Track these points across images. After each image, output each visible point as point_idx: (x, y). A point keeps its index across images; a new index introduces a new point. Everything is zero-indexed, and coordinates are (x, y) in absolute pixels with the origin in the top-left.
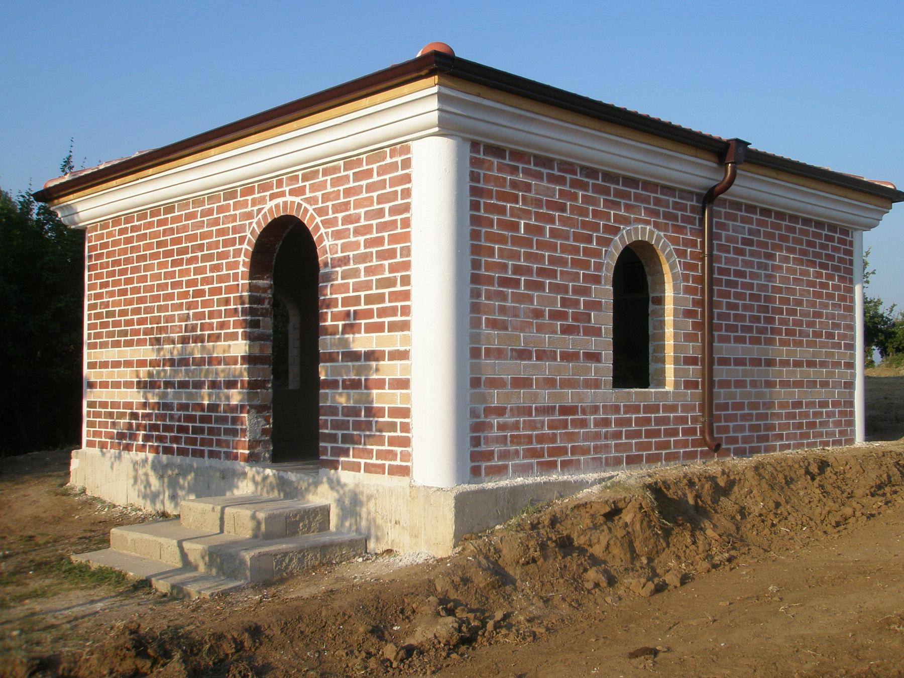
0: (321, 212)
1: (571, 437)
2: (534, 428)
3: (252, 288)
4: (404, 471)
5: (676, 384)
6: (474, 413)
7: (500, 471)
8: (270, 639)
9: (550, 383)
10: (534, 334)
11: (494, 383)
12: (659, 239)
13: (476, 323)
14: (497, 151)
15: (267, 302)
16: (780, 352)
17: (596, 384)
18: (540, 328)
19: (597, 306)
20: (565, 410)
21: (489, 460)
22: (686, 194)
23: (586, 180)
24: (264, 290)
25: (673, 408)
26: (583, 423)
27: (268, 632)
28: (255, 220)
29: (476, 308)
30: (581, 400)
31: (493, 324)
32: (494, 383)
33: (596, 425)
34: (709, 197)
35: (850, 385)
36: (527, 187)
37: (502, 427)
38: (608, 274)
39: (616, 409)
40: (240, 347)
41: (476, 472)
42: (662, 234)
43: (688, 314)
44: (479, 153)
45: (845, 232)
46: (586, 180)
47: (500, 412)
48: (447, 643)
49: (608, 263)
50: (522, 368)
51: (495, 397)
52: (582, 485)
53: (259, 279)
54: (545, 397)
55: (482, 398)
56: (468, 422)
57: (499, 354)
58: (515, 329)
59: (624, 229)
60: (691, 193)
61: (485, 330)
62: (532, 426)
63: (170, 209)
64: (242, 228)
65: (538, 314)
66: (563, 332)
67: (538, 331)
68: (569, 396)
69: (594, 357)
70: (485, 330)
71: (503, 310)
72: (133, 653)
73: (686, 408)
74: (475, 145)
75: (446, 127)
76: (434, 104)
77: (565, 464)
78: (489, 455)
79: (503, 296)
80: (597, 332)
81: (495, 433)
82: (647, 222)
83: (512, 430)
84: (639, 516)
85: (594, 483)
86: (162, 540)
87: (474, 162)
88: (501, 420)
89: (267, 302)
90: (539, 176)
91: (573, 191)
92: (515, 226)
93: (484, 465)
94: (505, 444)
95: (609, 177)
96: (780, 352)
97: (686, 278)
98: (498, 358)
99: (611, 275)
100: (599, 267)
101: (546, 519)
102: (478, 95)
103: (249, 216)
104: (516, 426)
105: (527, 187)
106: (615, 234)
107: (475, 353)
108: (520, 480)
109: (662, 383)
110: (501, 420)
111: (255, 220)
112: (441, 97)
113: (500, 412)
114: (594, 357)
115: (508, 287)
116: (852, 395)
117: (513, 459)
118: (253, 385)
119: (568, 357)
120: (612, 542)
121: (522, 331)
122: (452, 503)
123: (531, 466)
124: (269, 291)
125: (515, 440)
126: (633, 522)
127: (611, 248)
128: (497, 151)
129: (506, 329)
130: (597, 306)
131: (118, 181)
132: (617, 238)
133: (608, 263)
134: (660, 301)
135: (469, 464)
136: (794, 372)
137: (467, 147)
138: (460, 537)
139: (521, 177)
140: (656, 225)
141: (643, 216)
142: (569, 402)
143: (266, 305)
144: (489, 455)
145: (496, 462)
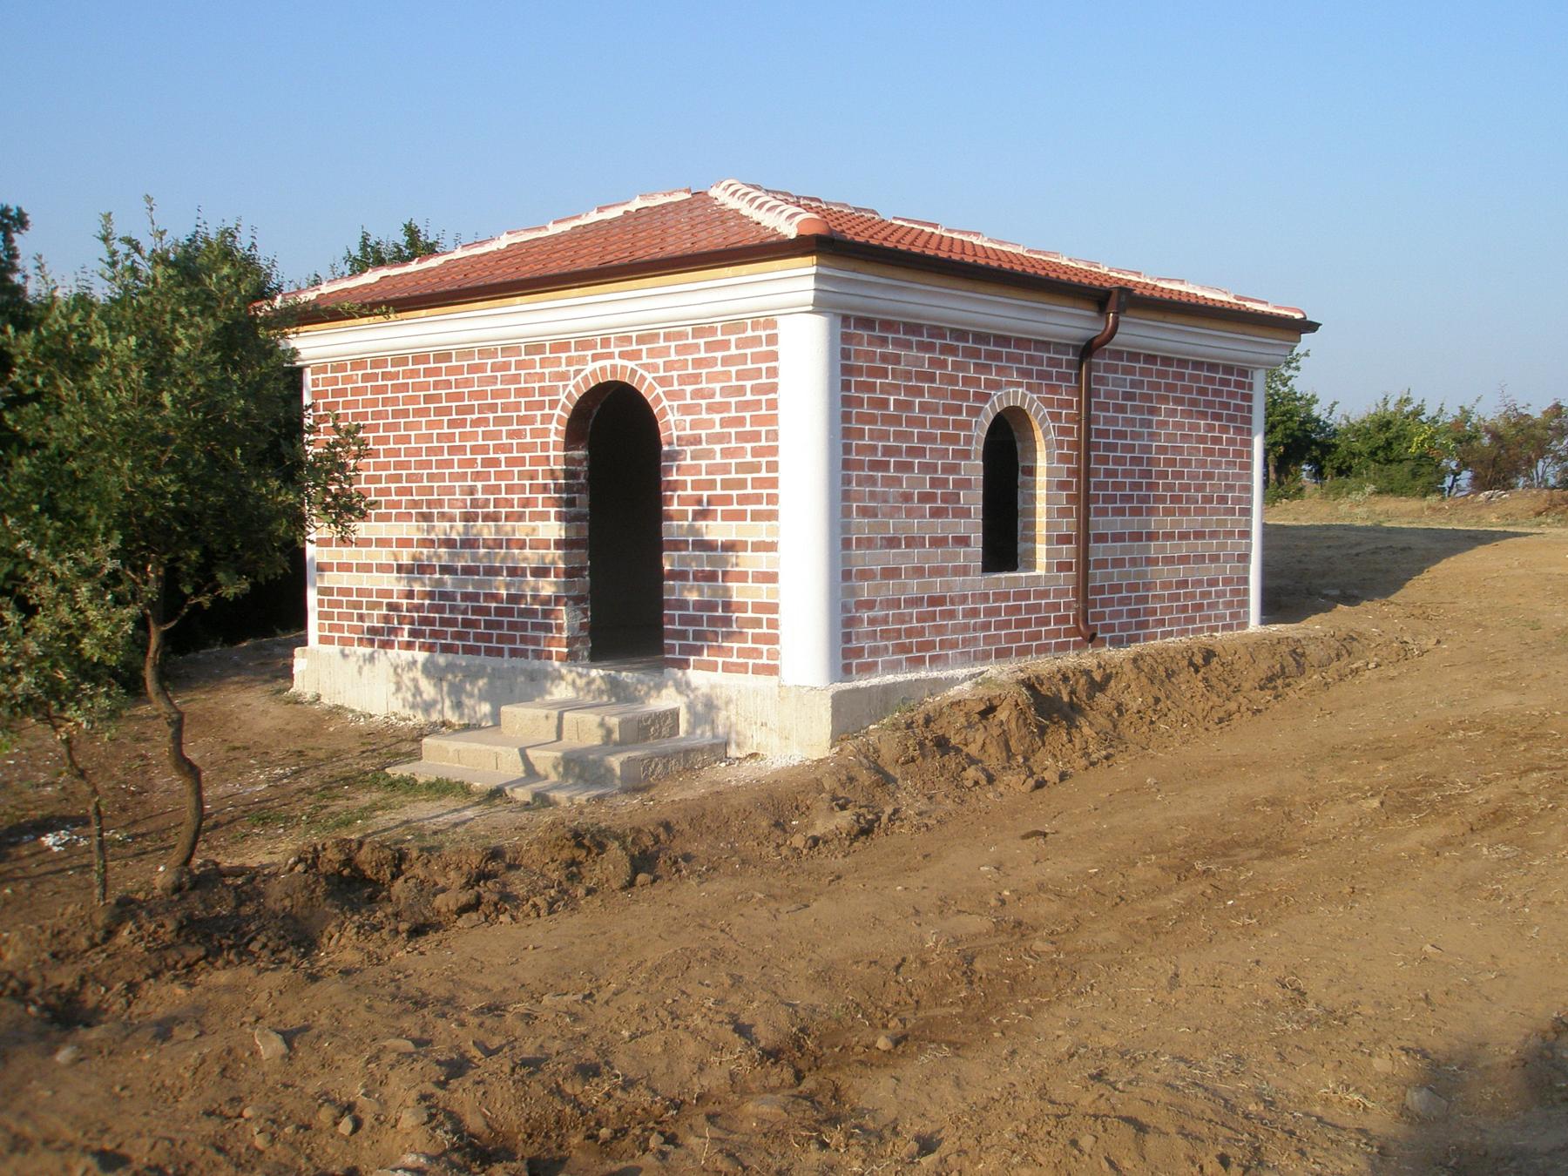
0: (663, 381)
1: (939, 630)
2: (903, 622)
3: (568, 461)
4: (772, 670)
5: (1049, 567)
6: (845, 608)
7: (869, 668)
8: (682, 833)
9: (919, 572)
10: (903, 519)
11: (865, 575)
12: (1032, 401)
13: (847, 512)
14: (866, 323)
15: (582, 475)
17: (965, 571)
18: (909, 513)
20: (934, 601)
21: (860, 657)
22: (1061, 347)
23: (956, 343)
24: (580, 462)
25: (1045, 594)
26: (951, 614)
27: (677, 827)
28: (572, 382)
29: (846, 496)
30: (950, 590)
31: (864, 512)
32: (865, 575)
33: (965, 616)
34: (1087, 350)
35: (1245, 558)
36: (896, 359)
37: (872, 621)
38: (978, 447)
39: (985, 597)
40: (553, 529)
41: (847, 669)
42: (1035, 396)
43: (1063, 485)
44: (849, 327)
46: (956, 343)
47: (870, 605)
48: (848, 834)
50: (891, 557)
51: (865, 590)
52: (952, 682)
53: (574, 449)
54: (914, 587)
55: (851, 592)
56: (840, 617)
57: (868, 543)
58: (884, 516)
59: (995, 395)
60: (1067, 345)
61: (856, 519)
62: (901, 619)
63: (446, 357)
64: (553, 390)
65: (907, 497)
66: (932, 516)
67: (907, 516)
68: (938, 585)
69: (963, 541)
70: (856, 519)
71: (873, 495)
72: (573, 843)
73: (1059, 593)
74: (845, 319)
75: (820, 306)
76: (810, 283)
77: (933, 659)
78: (859, 652)
79: (872, 481)
80: (966, 513)
81: (865, 628)
82: (1019, 385)
83: (881, 625)
84: (1015, 713)
85: (964, 680)
86: (498, 749)
87: (846, 338)
89: (582, 475)
90: (907, 345)
92: (884, 404)
93: (855, 662)
94: (875, 640)
95: (981, 338)
97: (1060, 445)
98: (868, 548)
99: (981, 448)
100: (968, 440)
101: (920, 720)
103: (564, 376)
104: (885, 620)
105: (896, 359)
106: (986, 402)
107: (847, 544)
108: (890, 678)
109: (1031, 566)
111: (572, 382)
112: (818, 277)
113: (870, 605)
114: (963, 541)
115: (878, 471)
116: (1247, 570)
118: (569, 573)
119: (938, 542)
120: (988, 741)
121: (892, 517)
122: (829, 703)
123: (899, 662)
124: (585, 463)
125: (885, 634)
126: (1008, 721)
127: (982, 418)
128: (866, 323)
129: (876, 516)
130: (964, 484)
134: (1031, 471)
135: (841, 662)
136: (1180, 546)
137: (839, 321)
138: (838, 737)
139: (890, 349)
140: (1030, 387)
141: (1015, 378)
142: (937, 592)
143: (582, 480)
144: (859, 652)
145: (866, 659)
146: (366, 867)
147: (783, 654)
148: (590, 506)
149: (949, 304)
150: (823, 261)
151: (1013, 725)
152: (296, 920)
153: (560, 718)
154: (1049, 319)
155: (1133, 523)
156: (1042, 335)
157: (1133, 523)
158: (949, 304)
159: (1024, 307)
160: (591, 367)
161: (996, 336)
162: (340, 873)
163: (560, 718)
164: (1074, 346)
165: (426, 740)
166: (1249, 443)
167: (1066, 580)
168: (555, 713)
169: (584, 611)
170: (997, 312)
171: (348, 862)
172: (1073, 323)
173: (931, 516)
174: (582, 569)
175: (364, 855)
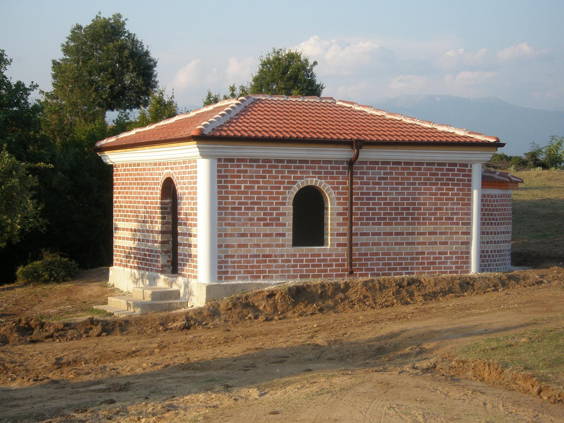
0: (177, 178)
2: (249, 263)
3: (162, 203)
4: (195, 277)
5: (331, 245)
7: (233, 278)
8: (131, 324)
9: (258, 246)
10: (249, 227)
12: (321, 184)
15: (169, 208)
17: (283, 246)
19: (284, 214)
20: (264, 256)
22: (342, 162)
23: (277, 164)
24: (168, 204)
25: (330, 255)
26: (275, 261)
27: (131, 322)
28: (162, 177)
30: (275, 252)
33: (282, 262)
34: (351, 163)
35: (468, 243)
37: (232, 262)
39: (295, 256)
40: (158, 227)
41: (220, 278)
42: (323, 181)
43: (339, 214)
45: (466, 165)
46: (277, 164)
48: (180, 327)
49: (290, 197)
50: (243, 240)
51: (230, 251)
52: (271, 285)
53: (165, 199)
54: (255, 251)
56: (217, 260)
59: (299, 182)
60: (344, 161)
62: (248, 262)
63: (139, 165)
64: (157, 179)
65: (251, 219)
66: (263, 226)
67: (251, 226)
68: (267, 251)
69: (283, 235)
72: (90, 323)
74: (219, 160)
75: (203, 156)
76: (197, 150)
77: (264, 277)
80: (284, 225)
82: (315, 177)
84: (280, 296)
85: (275, 284)
86: (121, 301)
88: (232, 260)
89: (169, 208)
91: (270, 169)
92: (239, 187)
97: (338, 199)
98: (231, 237)
99: (292, 201)
100: (284, 198)
101: (244, 296)
102: (215, 145)
103: (160, 174)
104: (240, 262)
108: (240, 282)
109: (327, 245)
110: (232, 260)
111: (162, 177)
112: (199, 148)
114: (283, 235)
115: (236, 210)
116: (469, 248)
117: (238, 274)
118: (162, 243)
119: (265, 235)
120: (266, 305)
121: (243, 226)
122: (205, 288)
123: (247, 277)
124: (170, 204)
126: (278, 299)
127: (292, 190)
129: (235, 226)
130: (284, 214)
131: (120, 150)
132: (295, 186)
133: (290, 197)
134: (327, 209)
135: (217, 275)
137: (216, 160)
138: (207, 300)
139: (242, 168)
141: (311, 175)
142: (267, 253)
143: (169, 210)
145: (229, 275)
146: (33, 326)
147: (199, 272)
148: (172, 219)
150: (199, 143)
151: (279, 301)
152: (6, 337)
153: (143, 291)
154: (324, 153)
155: (410, 229)
156: (326, 158)
157: (410, 229)
159: (307, 150)
160: (166, 171)
161: (299, 160)
162: (24, 327)
163: (143, 291)
164: (346, 161)
165: (109, 298)
166: (469, 195)
167: (344, 251)
168: (142, 290)
169: (169, 256)
170: (293, 152)
171: (27, 323)
172: (345, 154)
173: (263, 226)
174: (169, 241)
175: (32, 322)
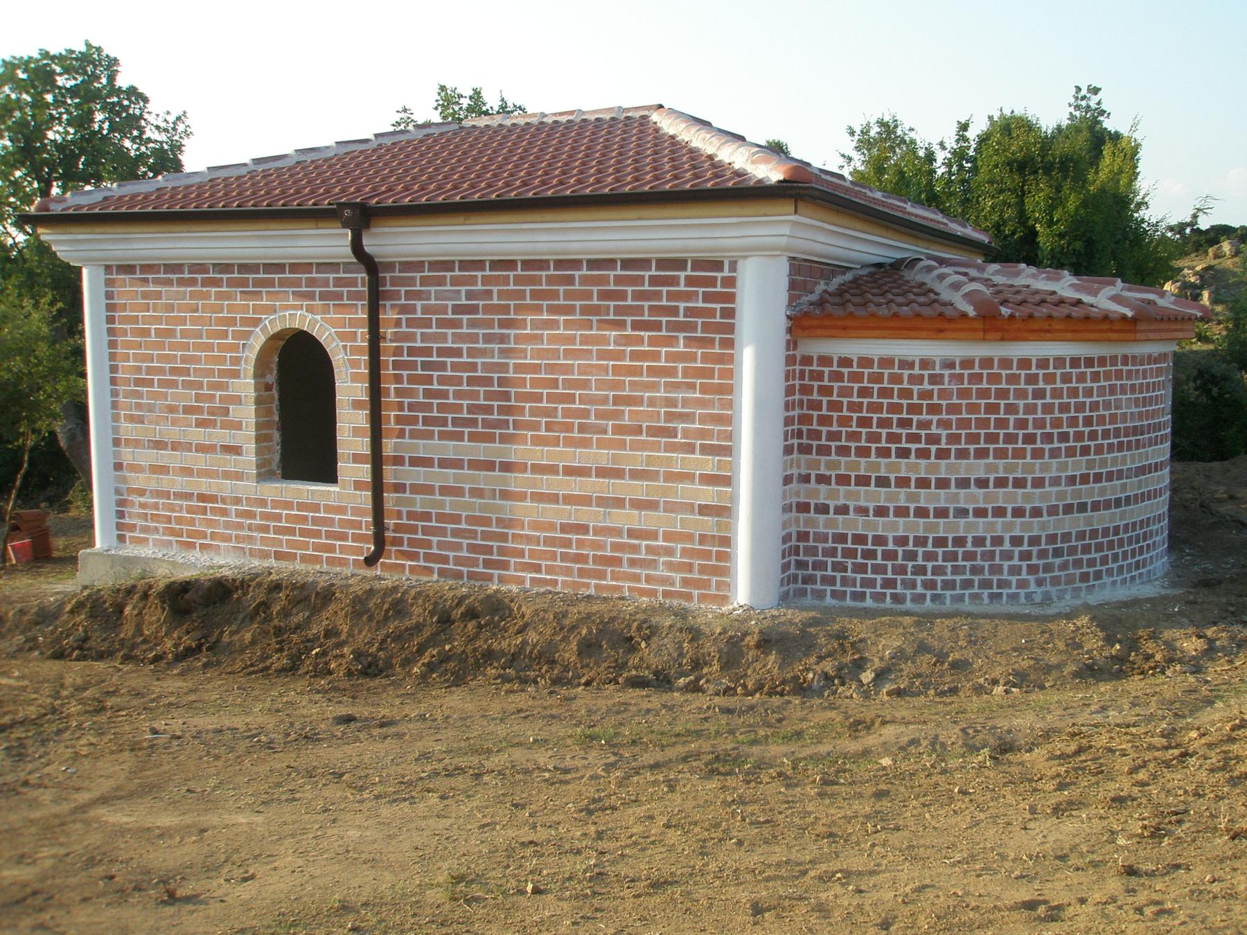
1: (210, 523)
2: (174, 511)
6: (118, 492)
11: (135, 468)
13: (116, 418)
14: (128, 269)
16: (518, 452)
17: (238, 476)
18: (174, 422)
19: (237, 400)
21: (132, 532)
23: (219, 276)
29: (115, 405)
31: (132, 419)
32: (135, 468)
36: (158, 295)
37: (142, 506)
38: (248, 367)
41: (121, 538)
42: (318, 317)
44: (112, 274)
45: (717, 265)
46: (219, 276)
47: (141, 492)
49: (247, 356)
55: (124, 480)
57: (137, 443)
58: (150, 423)
59: (267, 319)
61: (124, 424)
65: (172, 409)
68: (205, 485)
69: (236, 450)
70: (124, 424)
71: (139, 406)
73: (356, 511)
74: (108, 268)
78: (132, 528)
79: (139, 395)
80: (238, 426)
81: (137, 510)
82: (301, 307)
83: (152, 510)
87: (109, 283)
88: (142, 500)
90: (169, 282)
91: (204, 289)
93: (128, 535)
94: (147, 521)
95: (244, 268)
96: (518, 452)
100: (237, 361)
102: (71, 233)
104: (156, 506)
105: (158, 295)
106: (256, 326)
107: (116, 442)
110: (142, 500)
113: (141, 492)
114: (236, 450)
117: (153, 534)
121: (157, 424)
123: (170, 542)
125: (155, 517)
128: (128, 269)
129: (143, 423)
130: (237, 400)
132: (258, 330)
133: (247, 356)
137: (102, 270)
140: (310, 309)
142: (204, 490)
144: (132, 528)
149: (158, 246)
158: (158, 246)
